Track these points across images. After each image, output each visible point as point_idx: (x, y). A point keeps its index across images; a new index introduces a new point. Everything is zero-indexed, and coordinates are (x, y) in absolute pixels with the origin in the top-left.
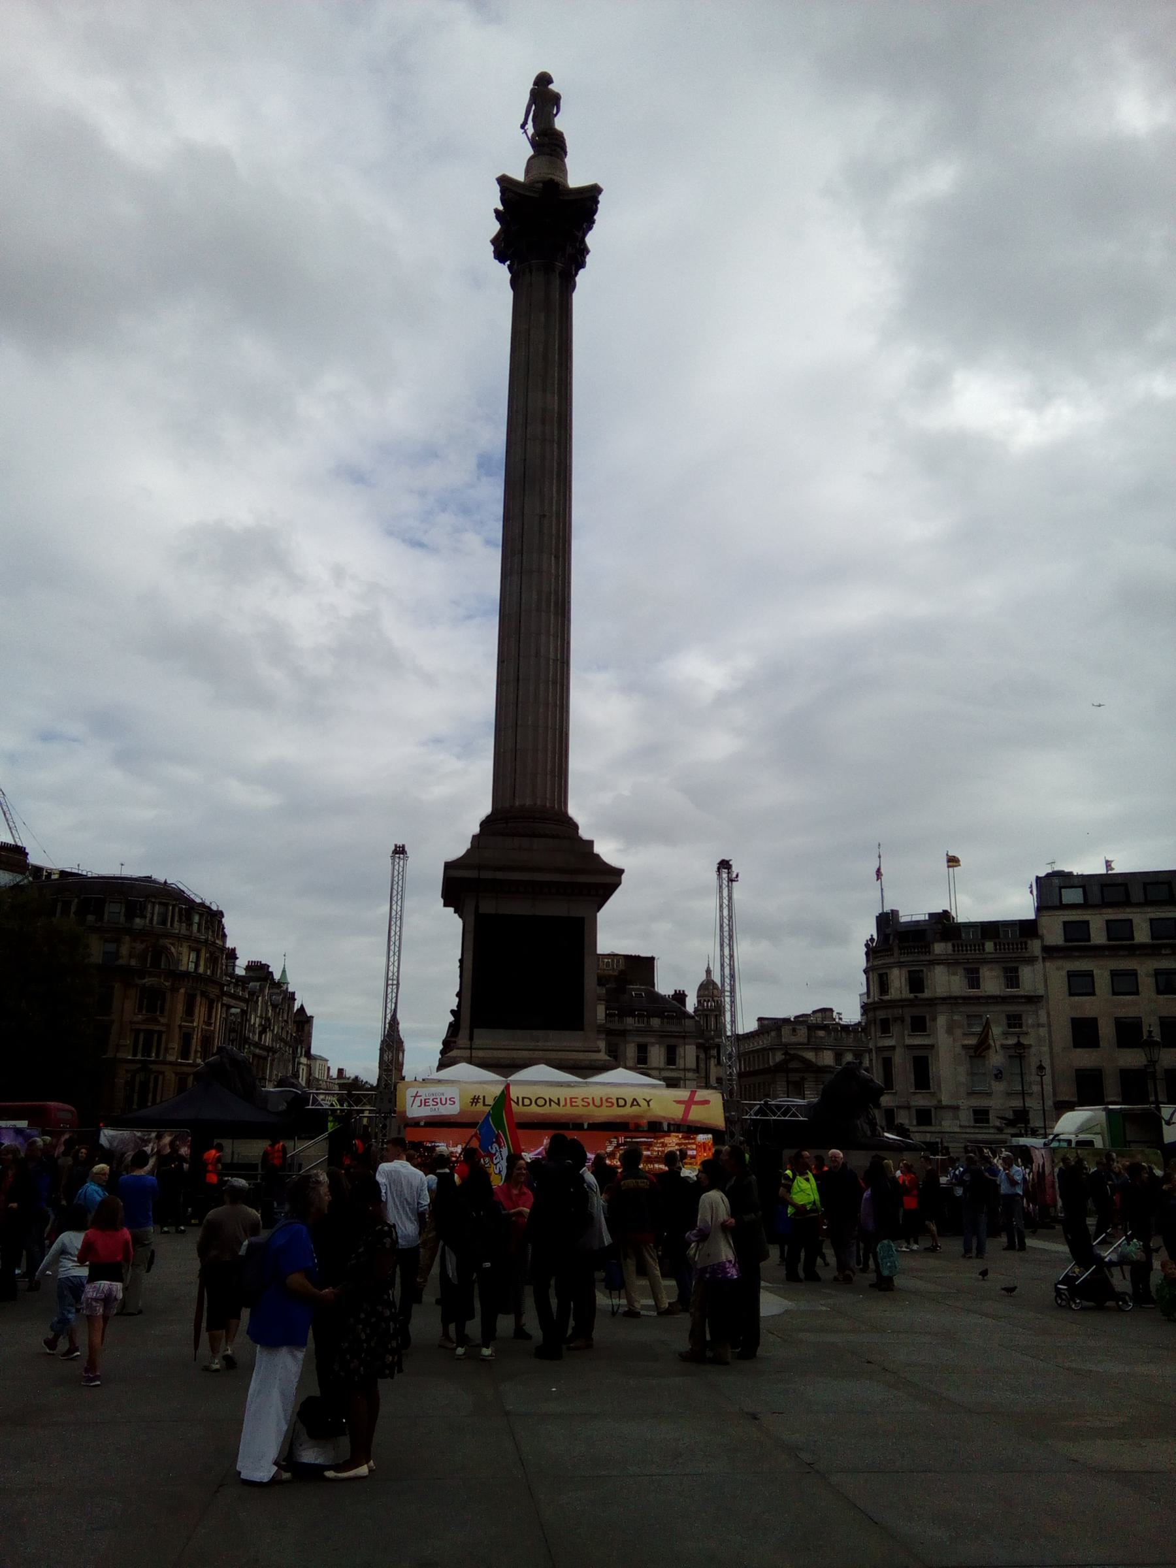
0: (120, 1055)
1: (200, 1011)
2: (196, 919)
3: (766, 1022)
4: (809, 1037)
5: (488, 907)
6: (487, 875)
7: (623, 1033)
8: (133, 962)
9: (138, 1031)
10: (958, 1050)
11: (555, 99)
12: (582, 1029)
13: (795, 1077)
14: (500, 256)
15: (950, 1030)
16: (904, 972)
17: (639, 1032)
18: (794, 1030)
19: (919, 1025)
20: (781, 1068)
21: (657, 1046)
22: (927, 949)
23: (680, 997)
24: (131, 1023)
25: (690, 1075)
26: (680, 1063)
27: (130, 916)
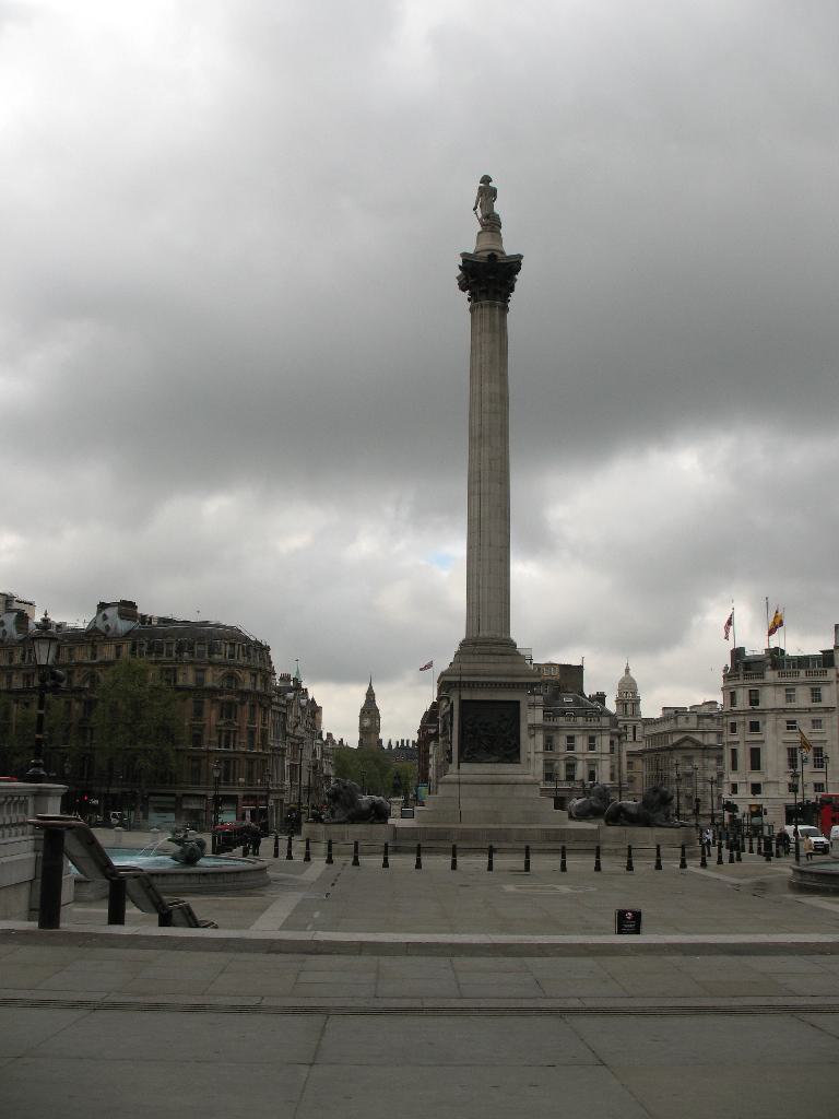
0: (211, 748)
1: (259, 716)
2: (252, 652)
3: (667, 712)
4: (698, 724)
5: (466, 696)
6: (464, 679)
7: (557, 729)
8: (215, 684)
9: (220, 731)
10: (780, 743)
11: (493, 193)
12: (519, 763)
13: (690, 753)
14: (463, 288)
15: (775, 730)
16: (746, 691)
17: (570, 728)
18: (687, 718)
19: (755, 727)
20: (676, 747)
21: (581, 738)
22: (761, 675)
23: (601, 698)
24: (217, 726)
25: (605, 757)
26: (598, 749)
27: (211, 653)
